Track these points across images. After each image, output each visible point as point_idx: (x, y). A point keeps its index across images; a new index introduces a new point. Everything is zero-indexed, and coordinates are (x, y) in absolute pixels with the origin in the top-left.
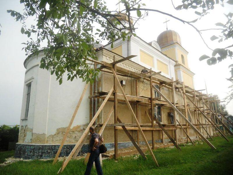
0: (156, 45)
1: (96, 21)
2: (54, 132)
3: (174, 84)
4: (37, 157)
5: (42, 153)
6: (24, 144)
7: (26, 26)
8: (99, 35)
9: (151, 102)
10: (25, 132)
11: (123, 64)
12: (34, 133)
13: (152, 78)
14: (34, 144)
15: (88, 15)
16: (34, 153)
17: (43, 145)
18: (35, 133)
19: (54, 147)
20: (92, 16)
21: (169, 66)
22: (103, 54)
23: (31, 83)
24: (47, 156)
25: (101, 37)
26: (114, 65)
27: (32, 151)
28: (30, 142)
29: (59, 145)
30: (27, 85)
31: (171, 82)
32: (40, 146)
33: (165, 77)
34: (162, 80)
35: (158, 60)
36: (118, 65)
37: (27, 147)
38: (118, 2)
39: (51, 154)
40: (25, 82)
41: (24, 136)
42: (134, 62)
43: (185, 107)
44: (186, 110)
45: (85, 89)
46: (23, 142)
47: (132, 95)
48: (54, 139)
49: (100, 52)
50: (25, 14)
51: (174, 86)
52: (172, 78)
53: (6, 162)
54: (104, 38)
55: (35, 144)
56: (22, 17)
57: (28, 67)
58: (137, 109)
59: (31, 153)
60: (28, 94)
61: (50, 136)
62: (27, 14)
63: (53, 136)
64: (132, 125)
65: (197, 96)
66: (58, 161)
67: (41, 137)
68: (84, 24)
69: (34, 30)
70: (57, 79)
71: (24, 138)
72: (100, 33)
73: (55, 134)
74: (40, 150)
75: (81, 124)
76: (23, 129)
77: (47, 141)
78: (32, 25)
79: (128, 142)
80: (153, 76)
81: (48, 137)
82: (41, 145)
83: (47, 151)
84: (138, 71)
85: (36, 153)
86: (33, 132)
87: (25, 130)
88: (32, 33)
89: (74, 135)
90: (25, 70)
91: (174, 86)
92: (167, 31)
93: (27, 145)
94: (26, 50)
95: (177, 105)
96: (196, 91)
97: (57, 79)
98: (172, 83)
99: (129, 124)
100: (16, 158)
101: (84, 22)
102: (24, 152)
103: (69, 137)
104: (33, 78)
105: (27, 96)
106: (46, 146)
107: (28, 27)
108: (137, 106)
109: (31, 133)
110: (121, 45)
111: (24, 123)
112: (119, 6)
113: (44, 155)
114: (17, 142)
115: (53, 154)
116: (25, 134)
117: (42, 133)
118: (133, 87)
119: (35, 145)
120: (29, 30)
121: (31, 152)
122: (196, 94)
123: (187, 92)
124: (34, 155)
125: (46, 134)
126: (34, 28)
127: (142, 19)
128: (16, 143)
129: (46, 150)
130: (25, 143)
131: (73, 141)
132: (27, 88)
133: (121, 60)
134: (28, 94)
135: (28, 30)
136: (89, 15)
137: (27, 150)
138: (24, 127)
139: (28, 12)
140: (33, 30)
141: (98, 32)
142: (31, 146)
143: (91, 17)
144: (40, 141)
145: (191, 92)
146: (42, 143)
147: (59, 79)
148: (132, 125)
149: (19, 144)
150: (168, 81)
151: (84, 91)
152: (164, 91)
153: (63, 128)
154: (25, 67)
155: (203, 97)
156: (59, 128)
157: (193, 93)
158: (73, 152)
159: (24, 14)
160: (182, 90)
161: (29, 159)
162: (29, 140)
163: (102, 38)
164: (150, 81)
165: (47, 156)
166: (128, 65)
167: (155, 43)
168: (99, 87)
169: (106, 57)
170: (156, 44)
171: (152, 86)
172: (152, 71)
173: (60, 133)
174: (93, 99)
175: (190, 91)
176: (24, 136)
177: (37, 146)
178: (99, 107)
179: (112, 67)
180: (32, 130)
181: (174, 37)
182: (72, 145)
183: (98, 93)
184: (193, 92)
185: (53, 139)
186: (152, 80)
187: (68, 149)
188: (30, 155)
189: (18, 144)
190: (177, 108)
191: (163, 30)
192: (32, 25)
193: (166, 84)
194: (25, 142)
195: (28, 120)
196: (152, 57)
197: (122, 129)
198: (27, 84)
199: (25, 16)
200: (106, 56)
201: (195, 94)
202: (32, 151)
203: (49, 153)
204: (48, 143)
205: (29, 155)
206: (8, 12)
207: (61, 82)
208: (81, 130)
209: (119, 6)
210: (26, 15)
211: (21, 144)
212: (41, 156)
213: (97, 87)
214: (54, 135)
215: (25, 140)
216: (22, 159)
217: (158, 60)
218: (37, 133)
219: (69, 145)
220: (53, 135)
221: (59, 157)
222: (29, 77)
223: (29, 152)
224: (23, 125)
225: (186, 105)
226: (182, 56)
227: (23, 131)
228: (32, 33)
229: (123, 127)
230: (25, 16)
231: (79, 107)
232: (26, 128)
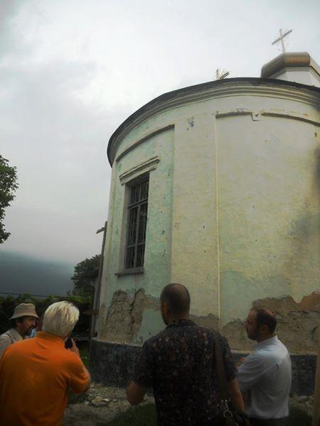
10: (136, 309)
30: (127, 184)
38: (278, 36)
41: (133, 322)
46: (131, 339)
53: (93, 401)
61: (231, 323)
71: (131, 329)
76: (124, 300)
81: (224, 328)
87: (132, 305)
103: (294, 328)
104: (158, 161)
111: (128, 285)
112: (283, 44)
116: (133, 314)
130: (137, 342)
131: (309, 343)
138: (132, 296)
153: (274, 299)
176: (133, 322)
195: (145, 272)
209: (283, 44)
215: (139, 334)
219: (303, 357)
232: (140, 296)
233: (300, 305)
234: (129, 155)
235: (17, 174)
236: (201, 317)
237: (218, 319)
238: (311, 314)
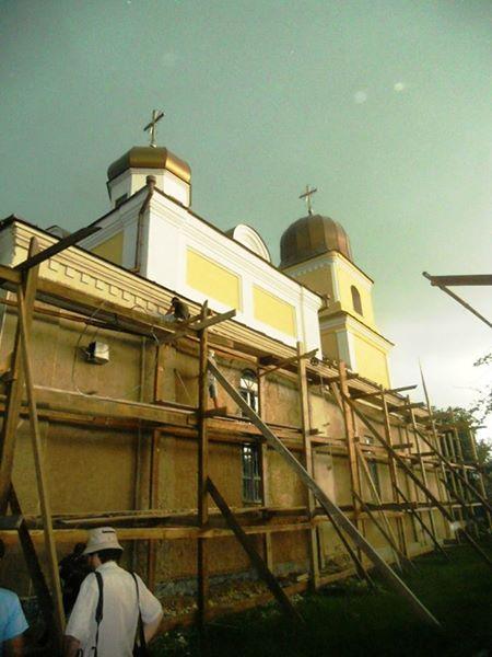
3: (304, 364)
9: (199, 427)
13: (205, 335)
21: (298, 308)
22: (18, 241)
31: (295, 358)
33: (281, 343)
34: (266, 350)
35: (256, 287)
36: (49, 271)
42: (154, 283)
43: (348, 445)
44: (353, 455)
47: (139, 401)
51: (303, 372)
52: (298, 343)
58: (152, 451)
64: (130, 514)
65: (392, 408)
84: (151, 306)
91: (303, 372)
92: (307, 219)
95: (313, 438)
96: (392, 392)
99: (100, 514)
108: (153, 441)
110: (122, 233)
118: (143, 372)
122: (388, 399)
123: (356, 393)
133: (50, 249)
145: (373, 395)
148: (114, 515)
150: (287, 354)
155: (414, 411)
157: (379, 397)
160: (340, 386)
164: (201, 343)
166: (152, 300)
171: (205, 366)
172: (209, 312)
175: (369, 390)
179: (14, 277)
181: (328, 235)
184: (378, 394)
186: (207, 343)
190: (318, 448)
191: (297, 213)
193: (278, 366)
196: (237, 277)
200: (66, 266)
201: (385, 401)
217: (256, 287)
225: (351, 437)
226: (354, 289)
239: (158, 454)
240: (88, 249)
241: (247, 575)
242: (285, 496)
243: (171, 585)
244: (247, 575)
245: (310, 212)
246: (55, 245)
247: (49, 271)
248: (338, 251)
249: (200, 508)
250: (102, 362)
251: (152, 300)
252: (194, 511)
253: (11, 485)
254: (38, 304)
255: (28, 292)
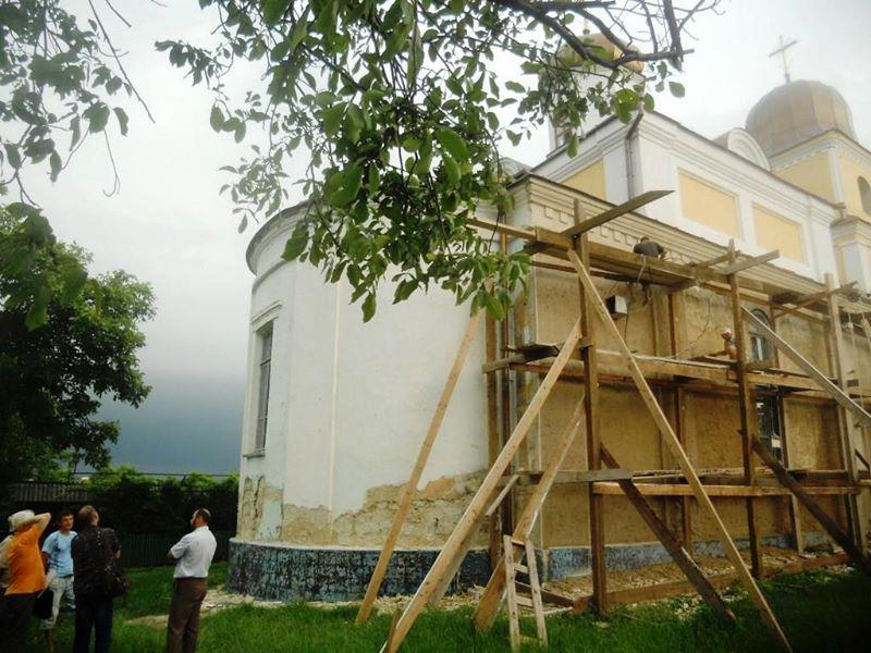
0: (744, 143)
1: (504, 46)
2: (357, 502)
3: (835, 304)
4: (302, 595)
5: (319, 578)
6: (254, 543)
7: (227, 99)
8: (517, 105)
9: (739, 380)
11: (613, 230)
12: (287, 505)
13: (737, 280)
14: (288, 545)
15: (467, 27)
16: (289, 578)
17: (321, 548)
18: (291, 503)
19: (359, 557)
20: (483, 29)
22: (532, 198)
23: (271, 322)
24: (336, 591)
25: (527, 115)
26: (579, 235)
27: (284, 570)
28: (276, 535)
29: (379, 553)
30: (258, 331)
32: (311, 555)
34: (780, 285)
35: (756, 207)
36: (596, 236)
37: (267, 555)
39: (351, 584)
40: (253, 323)
41: (257, 516)
42: (656, 222)
45: (467, 336)
46: (253, 536)
47: (655, 355)
48: (357, 528)
49: (520, 192)
50: (222, 52)
51: (836, 311)
52: (827, 275)
54: (540, 115)
55: (292, 547)
56: (211, 63)
57: (263, 268)
59: (282, 577)
60: (265, 365)
61: (342, 516)
62: (230, 49)
63: (354, 517)
64: (659, 474)
66: (377, 610)
67: (312, 519)
68: (456, 66)
69: (258, 109)
70: (355, 297)
72: (520, 97)
73: (363, 511)
74: (312, 570)
75: (458, 473)
76: (251, 490)
77: (335, 535)
78: (249, 94)
79: (645, 546)
80: (743, 273)
81: (336, 521)
82: (312, 551)
83: (336, 573)
85: (298, 579)
86: (285, 503)
87: (256, 494)
88: (251, 125)
89: (431, 515)
90: (251, 278)
91: (836, 311)
93: (266, 548)
94: (234, 192)
95: (854, 390)
97: (355, 297)
98: (829, 296)
99: (646, 472)
100: (229, 592)
101: (453, 59)
102: (258, 574)
105: (259, 369)
106: (329, 552)
107: (235, 104)
108: (677, 396)
109: (277, 505)
110: (602, 159)
113: (324, 588)
114: (234, 536)
115: (358, 584)
117: (317, 507)
119: (291, 551)
120: (239, 112)
121: (278, 574)
124: (289, 587)
125: (330, 509)
126: (258, 104)
127: (710, 10)
128: (231, 540)
129: (333, 570)
131: (430, 536)
132: (261, 341)
133: (602, 215)
134: (265, 365)
135: (234, 115)
136: (472, 25)
137: (265, 565)
139: (234, 45)
140: (252, 110)
141: (511, 94)
142: (279, 550)
143: (480, 34)
144: (310, 534)
146: (317, 544)
147: (362, 299)
148: (659, 474)
149: (241, 545)
151: (463, 344)
152: (791, 332)
154: (252, 268)
156: (377, 489)
158: (428, 583)
159: (220, 54)
161: (273, 597)
162: (273, 529)
163: (531, 119)
164: (733, 291)
165: (336, 591)
167: (745, 140)
168: (522, 326)
169: (542, 209)
170: (745, 140)
172: (738, 254)
173: (379, 505)
174: (498, 373)
177: (301, 551)
178: (523, 404)
179: (567, 244)
180: (281, 492)
182: (424, 552)
183: (518, 351)
185: (353, 527)
187: (412, 565)
188: (275, 586)
189: (235, 545)
192: (249, 94)
194: (258, 536)
195: (267, 457)
196: (733, 197)
197: (622, 492)
198: (259, 330)
199: (222, 59)
200: (545, 206)
202: (284, 570)
203: (344, 579)
204: (336, 543)
205: (272, 586)
206: (158, 49)
207: (369, 310)
208: (459, 496)
210: (227, 54)
211: (245, 545)
212: (316, 590)
213: (515, 329)
214: (359, 514)
215: (260, 531)
216: (249, 599)
217: (756, 207)
218: (298, 505)
219: (414, 553)
220: (354, 512)
221: (380, 595)
222: (265, 302)
223: (273, 576)
224: (250, 476)
227: (252, 498)
228: (251, 125)
229: (627, 484)
230: (222, 59)
231: (446, 407)
232: (262, 485)
233: (422, 492)
234: (271, 281)
235: (154, 292)
236: (312, 510)
237: (328, 511)
238: (440, 503)
239: (683, 412)
240: (558, 182)
241: (774, 542)
242: (807, 457)
243: (704, 546)
244: (774, 542)
245: (787, 76)
246: (609, 212)
247: (596, 236)
248: (838, 131)
249: (747, 466)
250: (622, 315)
251: (619, 229)
252: (740, 471)
253: (601, 444)
254: (592, 269)
255: (584, 257)
